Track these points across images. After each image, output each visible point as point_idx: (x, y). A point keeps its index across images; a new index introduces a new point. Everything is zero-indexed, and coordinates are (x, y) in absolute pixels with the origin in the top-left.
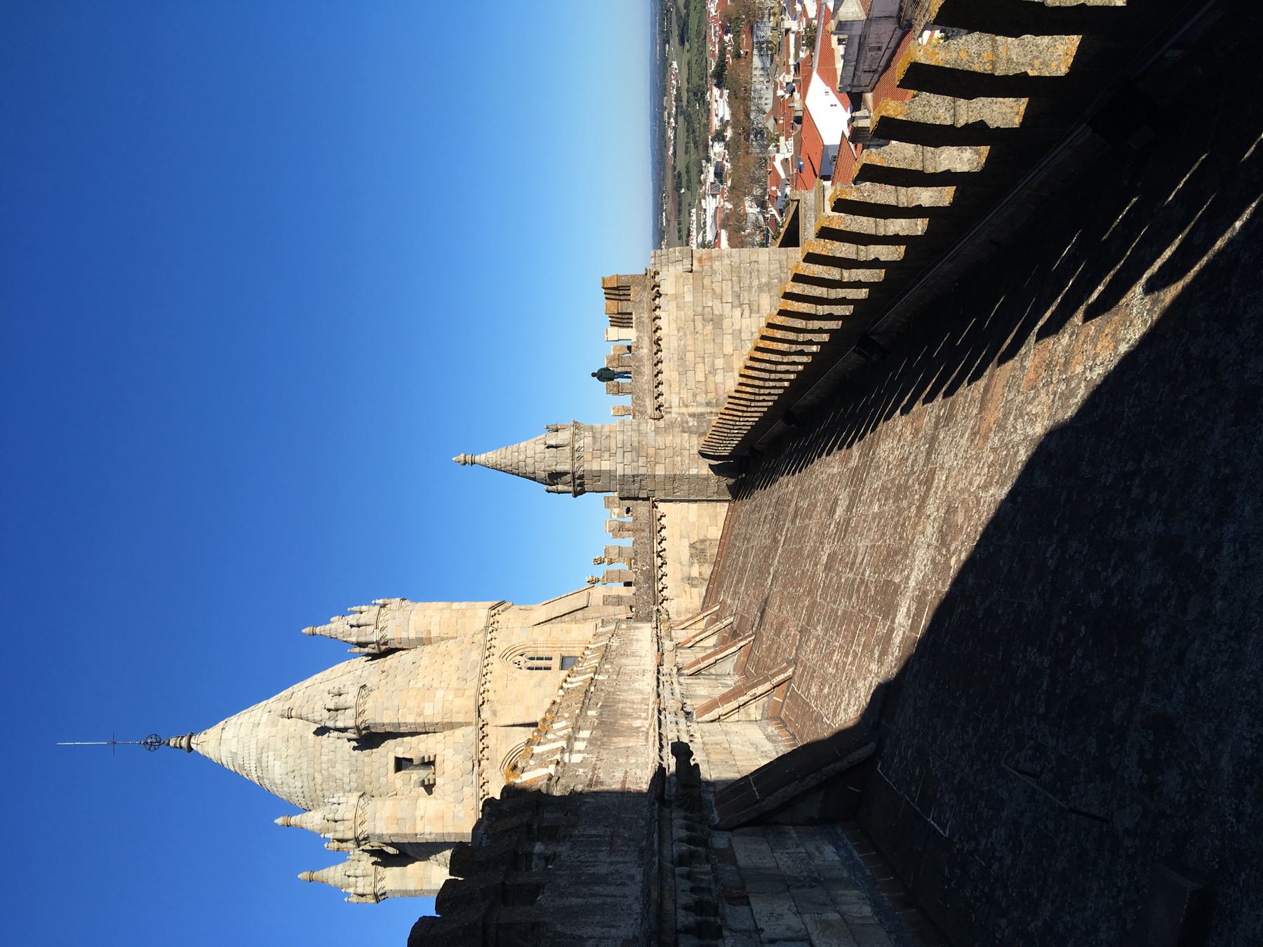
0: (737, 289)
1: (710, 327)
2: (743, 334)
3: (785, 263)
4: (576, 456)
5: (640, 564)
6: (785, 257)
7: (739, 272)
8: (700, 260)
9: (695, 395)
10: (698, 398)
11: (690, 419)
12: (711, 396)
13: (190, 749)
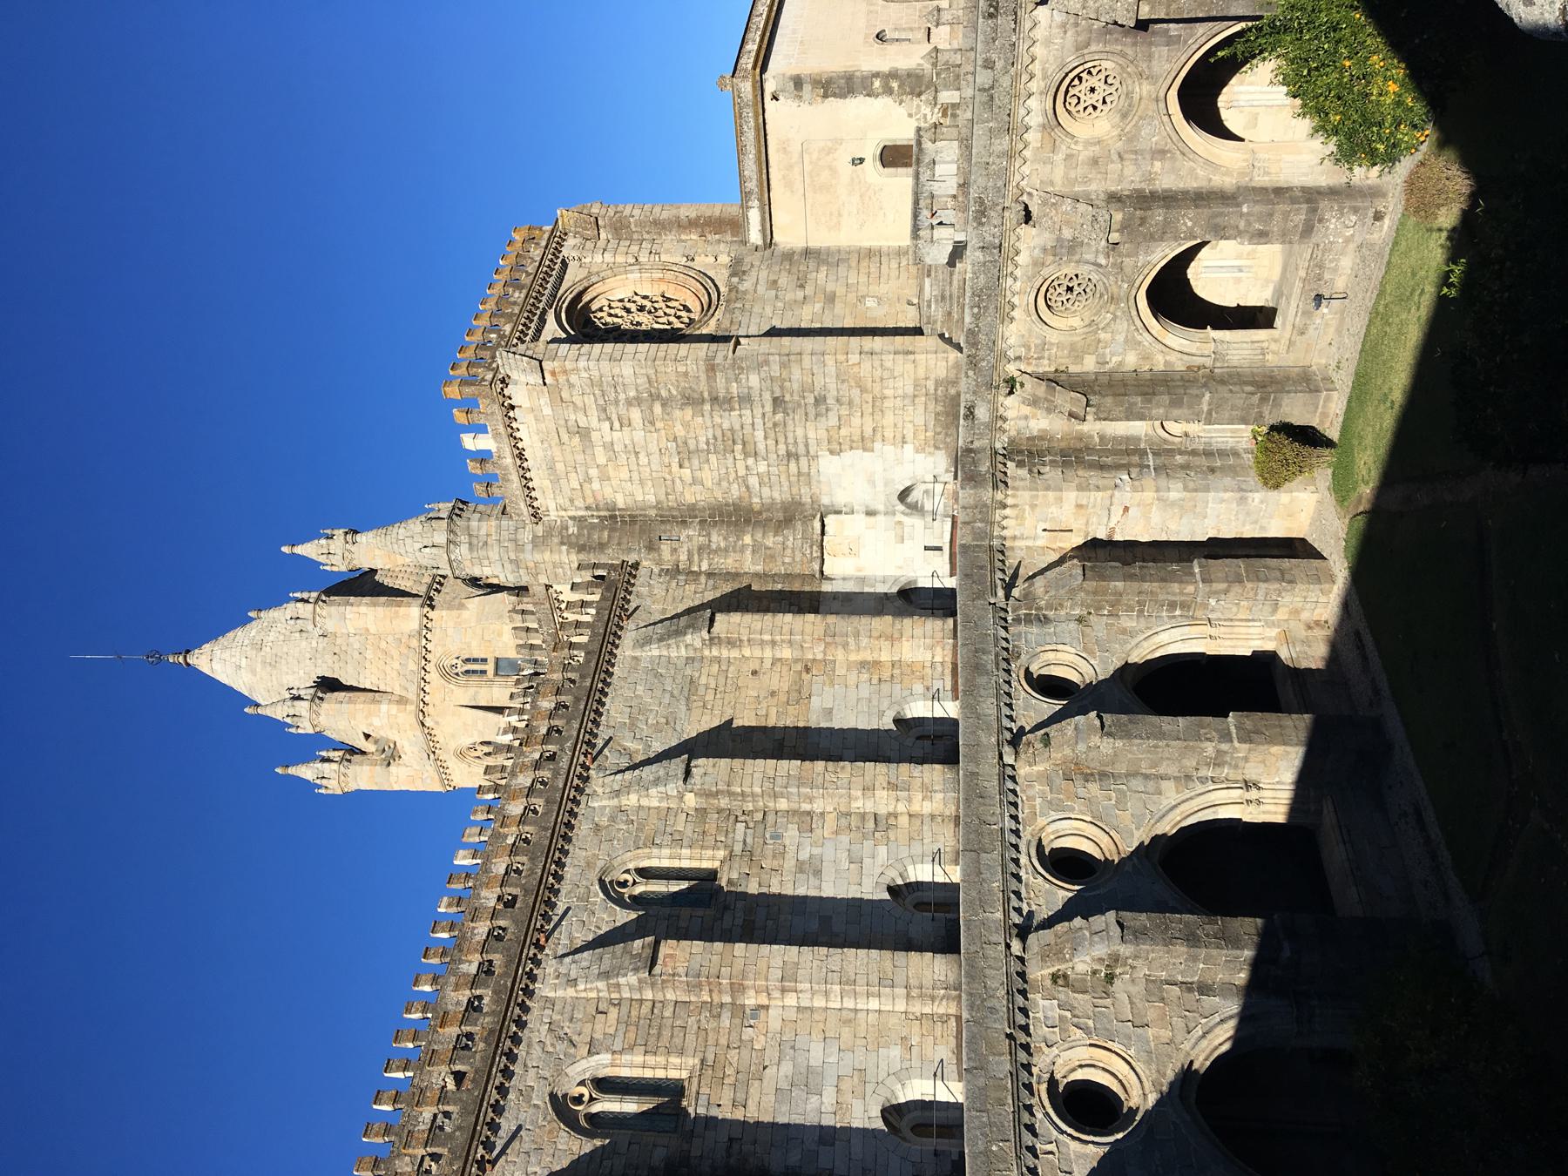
0: (601, 402)
1: (576, 439)
2: (615, 446)
4: (455, 564)
5: (545, 629)
6: (651, 372)
7: (601, 385)
8: (553, 373)
9: (572, 501)
10: (576, 503)
11: (571, 523)
12: (590, 501)
13: (188, 665)
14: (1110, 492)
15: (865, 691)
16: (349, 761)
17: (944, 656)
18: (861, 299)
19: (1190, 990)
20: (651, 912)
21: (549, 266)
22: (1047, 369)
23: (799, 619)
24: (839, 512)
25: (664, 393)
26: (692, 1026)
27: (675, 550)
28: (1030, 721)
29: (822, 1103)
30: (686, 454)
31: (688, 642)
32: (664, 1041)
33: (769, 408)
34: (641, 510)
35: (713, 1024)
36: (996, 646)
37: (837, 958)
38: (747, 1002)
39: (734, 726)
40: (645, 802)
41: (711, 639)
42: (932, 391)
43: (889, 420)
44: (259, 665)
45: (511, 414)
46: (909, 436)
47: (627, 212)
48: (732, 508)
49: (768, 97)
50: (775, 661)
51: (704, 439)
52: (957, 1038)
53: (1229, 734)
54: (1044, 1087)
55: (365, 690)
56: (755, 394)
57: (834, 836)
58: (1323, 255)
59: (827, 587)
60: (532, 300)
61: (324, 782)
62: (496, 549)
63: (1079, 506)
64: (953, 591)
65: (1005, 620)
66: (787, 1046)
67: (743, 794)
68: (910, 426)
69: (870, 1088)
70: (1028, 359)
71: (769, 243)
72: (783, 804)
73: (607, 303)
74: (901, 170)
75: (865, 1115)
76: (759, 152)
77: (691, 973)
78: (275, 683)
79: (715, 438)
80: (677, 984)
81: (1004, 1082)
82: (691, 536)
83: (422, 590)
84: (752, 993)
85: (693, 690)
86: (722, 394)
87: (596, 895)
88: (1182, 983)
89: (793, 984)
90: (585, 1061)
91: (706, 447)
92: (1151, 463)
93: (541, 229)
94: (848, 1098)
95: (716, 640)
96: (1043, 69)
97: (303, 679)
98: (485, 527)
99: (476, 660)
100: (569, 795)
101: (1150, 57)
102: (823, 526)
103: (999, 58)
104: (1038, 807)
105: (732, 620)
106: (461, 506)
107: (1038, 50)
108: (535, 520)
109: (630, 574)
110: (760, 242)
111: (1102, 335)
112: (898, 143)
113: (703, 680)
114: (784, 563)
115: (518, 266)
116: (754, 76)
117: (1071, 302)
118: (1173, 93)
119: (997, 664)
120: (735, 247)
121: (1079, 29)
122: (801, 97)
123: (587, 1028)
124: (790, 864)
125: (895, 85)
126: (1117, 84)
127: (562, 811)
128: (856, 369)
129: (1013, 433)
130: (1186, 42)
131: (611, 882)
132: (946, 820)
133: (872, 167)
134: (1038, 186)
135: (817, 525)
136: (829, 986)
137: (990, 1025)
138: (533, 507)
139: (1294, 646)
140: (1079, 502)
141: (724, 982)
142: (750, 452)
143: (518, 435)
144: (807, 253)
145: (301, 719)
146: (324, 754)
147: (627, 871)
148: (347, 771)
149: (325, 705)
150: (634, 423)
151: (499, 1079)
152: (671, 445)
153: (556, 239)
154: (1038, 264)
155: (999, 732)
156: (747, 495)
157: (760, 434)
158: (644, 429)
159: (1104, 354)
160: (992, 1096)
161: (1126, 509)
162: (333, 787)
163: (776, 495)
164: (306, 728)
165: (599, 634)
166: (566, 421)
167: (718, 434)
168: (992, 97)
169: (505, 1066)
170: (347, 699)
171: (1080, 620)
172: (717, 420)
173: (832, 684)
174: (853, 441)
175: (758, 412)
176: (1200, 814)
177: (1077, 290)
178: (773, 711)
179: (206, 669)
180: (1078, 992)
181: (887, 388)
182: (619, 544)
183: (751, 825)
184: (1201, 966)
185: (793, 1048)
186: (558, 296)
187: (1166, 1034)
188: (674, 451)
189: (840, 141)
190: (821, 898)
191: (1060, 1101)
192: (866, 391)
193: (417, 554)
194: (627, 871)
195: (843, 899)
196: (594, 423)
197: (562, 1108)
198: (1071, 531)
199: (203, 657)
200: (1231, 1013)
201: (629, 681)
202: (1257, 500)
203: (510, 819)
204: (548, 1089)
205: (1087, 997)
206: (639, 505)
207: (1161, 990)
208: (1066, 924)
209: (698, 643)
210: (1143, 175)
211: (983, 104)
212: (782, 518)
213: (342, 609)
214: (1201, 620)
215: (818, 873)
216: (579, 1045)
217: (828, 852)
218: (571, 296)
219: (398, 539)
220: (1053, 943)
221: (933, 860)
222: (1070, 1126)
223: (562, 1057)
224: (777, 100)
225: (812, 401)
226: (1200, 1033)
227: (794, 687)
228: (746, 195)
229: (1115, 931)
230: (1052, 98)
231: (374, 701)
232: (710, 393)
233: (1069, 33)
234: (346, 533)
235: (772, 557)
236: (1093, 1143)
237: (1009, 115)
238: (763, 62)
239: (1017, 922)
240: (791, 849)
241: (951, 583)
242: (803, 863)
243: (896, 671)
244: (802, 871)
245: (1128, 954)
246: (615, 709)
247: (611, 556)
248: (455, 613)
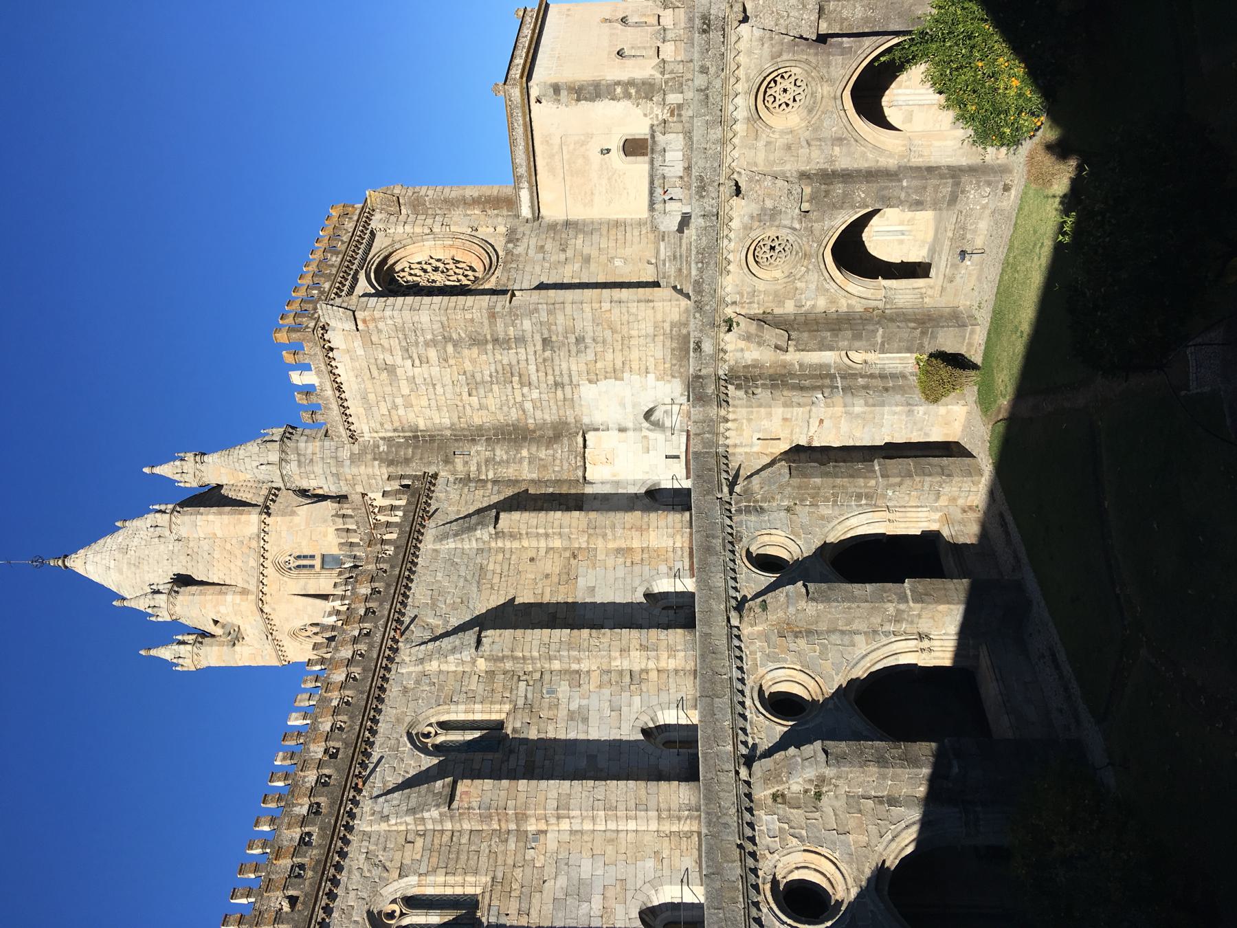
0: (404, 344)
1: (385, 375)
2: (416, 379)
3: (446, 323)
4: (286, 478)
5: (362, 529)
6: (444, 319)
7: (404, 330)
8: (364, 321)
9: (382, 425)
10: (386, 426)
11: (381, 442)
12: (398, 424)
13: (66, 567)
14: (808, 408)
15: (621, 572)
16: (201, 643)
17: (683, 543)
18: (611, 260)
19: (881, 803)
20: (450, 757)
21: (360, 236)
22: (757, 311)
23: (567, 515)
24: (597, 430)
25: (455, 336)
26: (484, 851)
27: (467, 462)
28: (751, 591)
29: (591, 908)
30: (473, 384)
31: (478, 536)
33: (539, 347)
34: (439, 430)
35: (502, 848)
36: (723, 532)
38: (529, 829)
39: (516, 603)
40: (444, 667)
41: (497, 533)
42: (668, 332)
43: (635, 355)
44: (125, 566)
45: (331, 355)
46: (651, 368)
47: (423, 192)
48: (512, 428)
49: (533, 100)
50: (548, 550)
51: (488, 372)
53: (906, 596)
54: (768, 886)
55: (213, 584)
56: (528, 335)
57: (598, 690)
58: (965, 219)
59: (589, 490)
60: (346, 263)
61: (180, 661)
62: (320, 465)
63: (785, 420)
64: (689, 490)
65: (730, 512)
66: (562, 863)
67: (524, 658)
68: (652, 359)
69: (629, 894)
70: (742, 303)
71: (537, 216)
72: (556, 665)
73: (408, 265)
74: (640, 159)
76: (527, 144)
77: (483, 806)
78: (138, 580)
79: (497, 372)
80: (471, 816)
81: (736, 884)
82: (479, 451)
83: (260, 501)
84: (533, 820)
85: (482, 575)
86: (501, 337)
87: (405, 745)
88: (875, 797)
89: (566, 812)
90: (396, 883)
91: (489, 379)
92: (839, 385)
93: (353, 207)
94: (611, 903)
95: (501, 534)
96: (746, 74)
97: (162, 577)
98: (309, 447)
99: (305, 557)
100: (381, 663)
101: (828, 65)
102: (585, 440)
103: (712, 66)
104: (759, 659)
105: (513, 518)
106: (291, 431)
107: (742, 59)
108: (353, 441)
109: (430, 483)
110: (530, 216)
111: (799, 284)
112: (637, 137)
113: (491, 567)
114: (554, 471)
115: (335, 236)
116: (521, 83)
117: (774, 258)
118: (847, 93)
119: (724, 546)
120: (510, 220)
121: (773, 42)
122: (559, 100)
124: (562, 713)
125: (633, 91)
126: (804, 87)
127: (376, 677)
128: (608, 315)
129: (732, 363)
130: (856, 52)
131: (417, 734)
132: (687, 674)
133: (617, 156)
134: (745, 167)
135: (580, 440)
136: (595, 812)
137: (725, 837)
138: (350, 430)
139: (953, 526)
140: (785, 416)
141: (510, 812)
142: (526, 382)
143: (336, 371)
144: (567, 224)
145: (161, 609)
146: (180, 637)
147: (430, 725)
148: (199, 651)
149: (180, 597)
150: (431, 361)
151: (325, 901)
152: (462, 378)
153: (366, 214)
154: (747, 228)
156: (523, 417)
157: (532, 368)
158: (439, 366)
159: (800, 299)
160: (727, 895)
161: (821, 421)
162: (188, 665)
163: (547, 417)
164: (164, 617)
165: (406, 533)
166: (376, 360)
167: (500, 368)
168: (707, 96)
169: (330, 890)
170: (198, 592)
171: (788, 510)
172: (498, 357)
173: (594, 567)
174: (607, 372)
175: (531, 350)
176: (885, 661)
177: (778, 249)
178: (548, 590)
179: (81, 571)
180: (794, 808)
181: (633, 329)
182: (421, 459)
183: (531, 683)
184: (890, 782)
185: (567, 864)
186: (368, 259)
187: (863, 839)
188: (464, 382)
189: (590, 136)
190: (588, 740)
191: (781, 897)
192: (617, 332)
193: (255, 470)
194: (430, 725)
196: (399, 361)
198: (779, 439)
199: (79, 560)
200: (913, 820)
201: (430, 569)
202: (921, 413)
203: (333, 686)
204: (366, 907)
205: (800, 811)
206: (437, 427)
207: (859, 803)
208: (783, 753)
209: (486, 537)
210: (826, 158)
211: (700, 101)
212: (552, 435)
213: (193, 517)
214: (882, 507)
215: (585, 720)
216: (391, 870)
217: (594, 703)
218: (379, 260)
219: (239, 459)
220: (772, 768)
222: (789, 917)
224: (540, 103)
225: (574, 340)
226: (890, 837)
227: (564, 571)
228: (517, 179)
230: (754, 97)
231: (221, 593)
232: (492, 335)
233: (766, 45)
234: (196, 455)
235: (545, 466)
237: (721, 110)
238: (528, 73)
239: (744, 753)
240: (564, 701)
241: (687, 484)
242: (573, 712)
243: (645, 556)
244: (572, 719)
245: (832, 776)
246: (419, 593)
247: (415, 469)
248: (288, 518)
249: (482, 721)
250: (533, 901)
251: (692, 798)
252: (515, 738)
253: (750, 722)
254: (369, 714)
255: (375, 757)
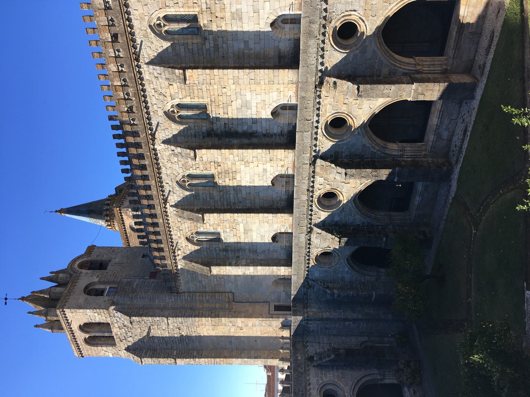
20: (176, 41)
26: (204, 89)
28: (331, 64)
29: (252, 112)
32: (196, 94)
35: (211, 88)
37: (253, 74)
52: (296, 88)
54: (316, 200)
69: (267, 106)
75: (266, 114)
77: (200, 83)
87: (151, 35)
94: (260, 110)
104: (328, 108)
119: (320, 31)
123: (168, 90)
124: (228, 15)
137: (303, 187)
139: (468, 8)
151: (145, 111)
155: (316, 74)
185: (240, 94)
187: (353, 186)
190: (243, 31)
195: (252, 31)
197: (169, 115)
204: (163, 111)
208: (330, 164)
215: (241, 19)
216: (167, 97)
220: (325, 166)
221: (290, 9)
223: (162, 100)
229: (344, 175)
236: (327, 212)
244: (233, 19)
249: (186, 15)
250: (229, 109)
251: (294, 78)
252: (206, 30)
253: (319, 140)
254: (125, 17)
255: (138, 41)
